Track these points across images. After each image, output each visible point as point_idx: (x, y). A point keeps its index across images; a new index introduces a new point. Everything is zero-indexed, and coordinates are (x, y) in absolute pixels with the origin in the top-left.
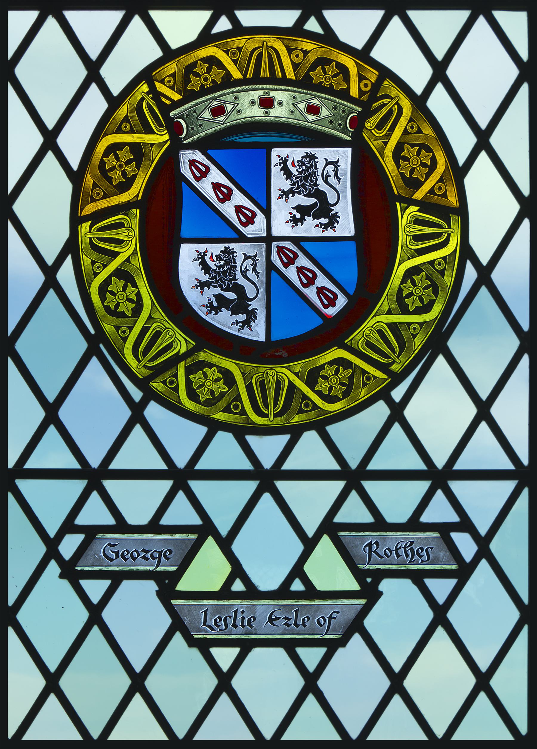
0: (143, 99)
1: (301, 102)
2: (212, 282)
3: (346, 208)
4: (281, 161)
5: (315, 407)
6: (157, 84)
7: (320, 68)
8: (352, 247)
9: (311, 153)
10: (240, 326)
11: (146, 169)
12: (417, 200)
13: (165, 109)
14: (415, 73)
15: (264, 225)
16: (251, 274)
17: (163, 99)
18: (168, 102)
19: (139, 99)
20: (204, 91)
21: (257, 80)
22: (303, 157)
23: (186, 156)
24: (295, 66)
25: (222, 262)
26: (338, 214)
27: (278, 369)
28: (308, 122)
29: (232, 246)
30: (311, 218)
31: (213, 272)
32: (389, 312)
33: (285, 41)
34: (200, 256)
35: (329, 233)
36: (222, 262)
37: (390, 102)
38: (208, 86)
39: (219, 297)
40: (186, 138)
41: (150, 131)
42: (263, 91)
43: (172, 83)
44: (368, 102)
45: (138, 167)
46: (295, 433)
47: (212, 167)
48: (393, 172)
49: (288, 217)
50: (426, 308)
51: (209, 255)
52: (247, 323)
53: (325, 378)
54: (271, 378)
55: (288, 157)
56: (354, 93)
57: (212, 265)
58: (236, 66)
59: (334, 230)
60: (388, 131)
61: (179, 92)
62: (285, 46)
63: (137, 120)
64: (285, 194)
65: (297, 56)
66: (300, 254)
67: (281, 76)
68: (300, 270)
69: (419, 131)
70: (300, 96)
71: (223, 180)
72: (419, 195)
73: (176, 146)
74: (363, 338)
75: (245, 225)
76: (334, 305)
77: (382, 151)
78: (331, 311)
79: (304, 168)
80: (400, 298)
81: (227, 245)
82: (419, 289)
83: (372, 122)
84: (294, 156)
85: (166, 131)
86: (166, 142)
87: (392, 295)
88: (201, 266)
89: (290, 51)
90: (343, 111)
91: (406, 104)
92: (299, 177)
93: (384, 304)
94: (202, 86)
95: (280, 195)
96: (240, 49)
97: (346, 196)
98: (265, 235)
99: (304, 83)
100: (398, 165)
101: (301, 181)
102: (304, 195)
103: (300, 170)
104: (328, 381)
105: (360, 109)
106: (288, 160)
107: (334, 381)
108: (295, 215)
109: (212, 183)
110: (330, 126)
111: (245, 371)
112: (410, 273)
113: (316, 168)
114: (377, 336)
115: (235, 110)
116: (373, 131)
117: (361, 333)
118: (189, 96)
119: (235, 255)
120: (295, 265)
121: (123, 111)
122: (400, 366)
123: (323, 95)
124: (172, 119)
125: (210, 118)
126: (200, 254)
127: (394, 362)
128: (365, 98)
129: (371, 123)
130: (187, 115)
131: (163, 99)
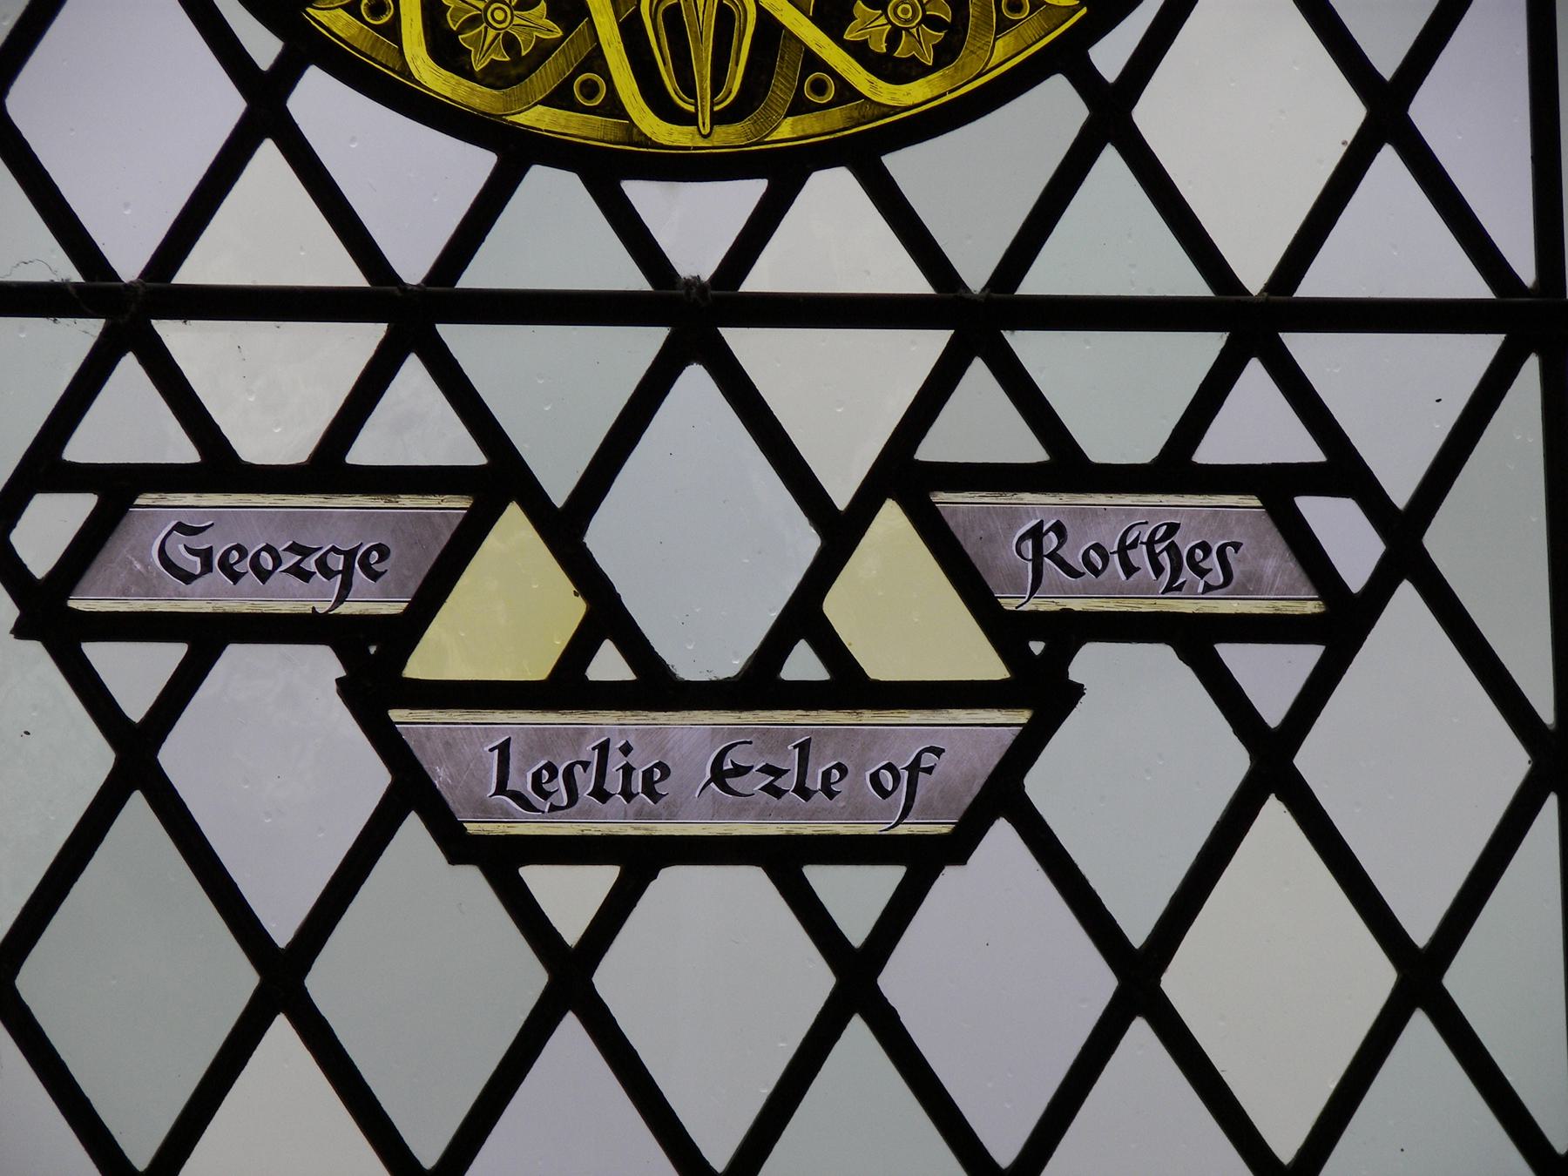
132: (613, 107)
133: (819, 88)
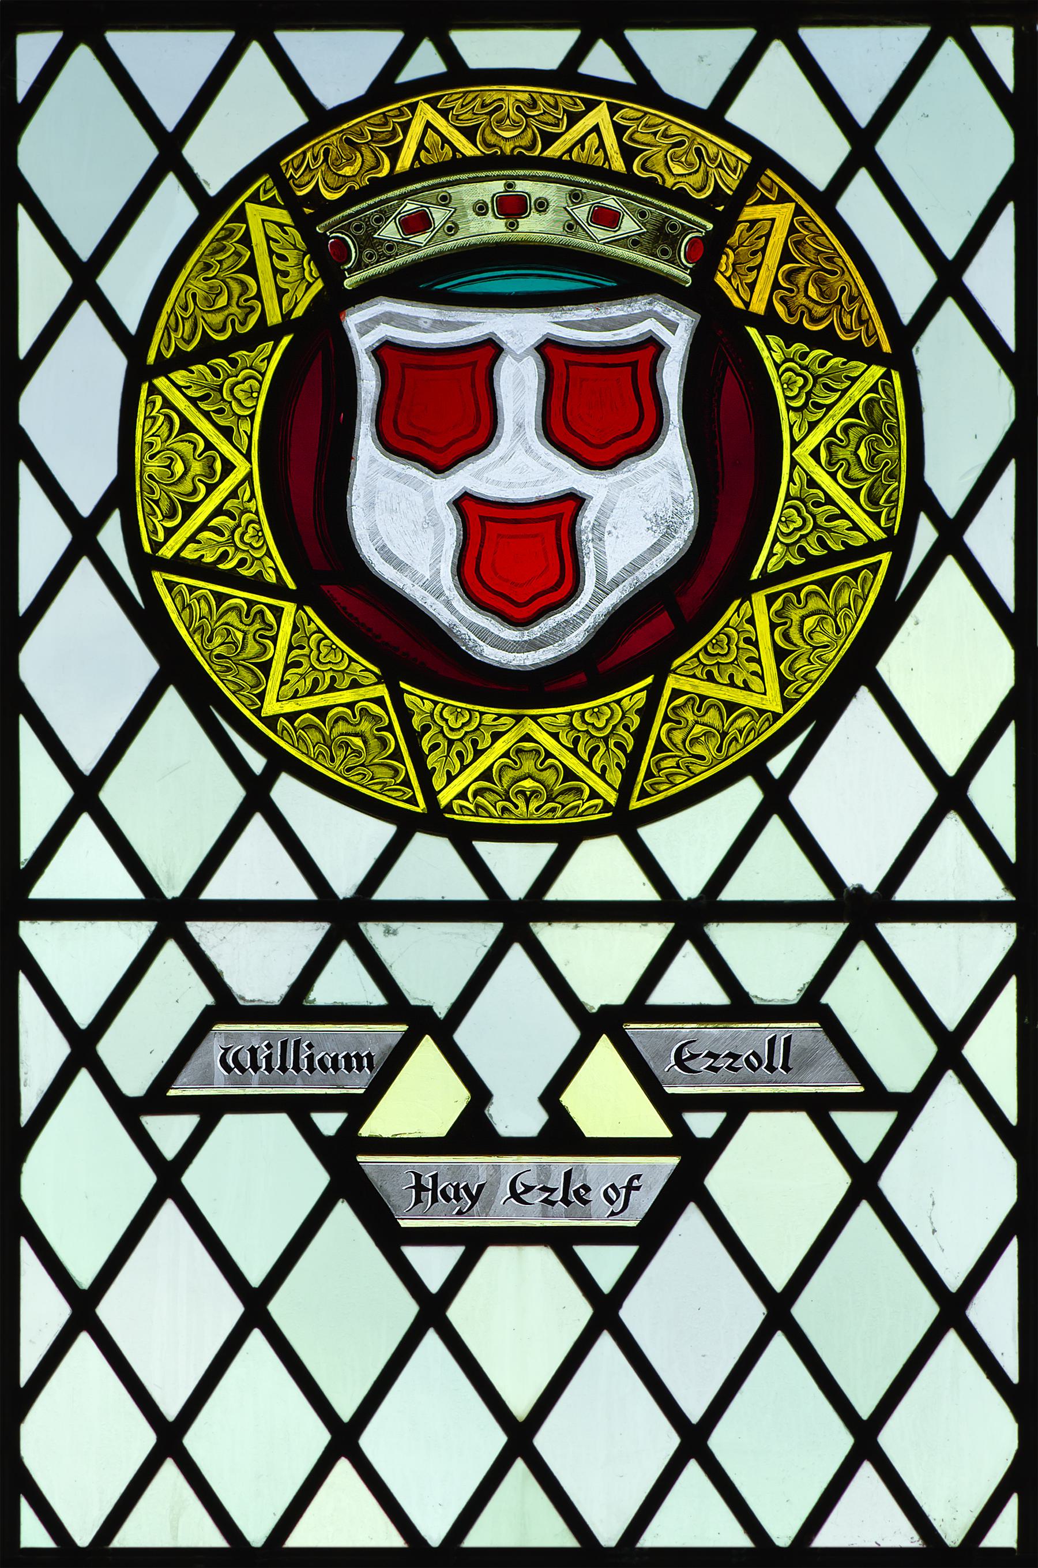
14: (815, 150)
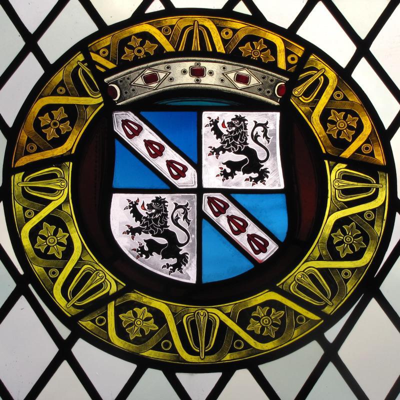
0: (78, 67)
1: (231, 72)
2: (144, 229)
3: (274, 165)
4: (212, 123)
5: (247, 346)
6: (92, 54)
7: (249, 44)
8: (281, 199)
9: (240, 116)
10: (171, 269)
11: (80, 126)
12: (345, 158)
13: (100, 76)
15: (195, 178)
16: (181, 222)
17: (98, 67)
18: (103, 70)
19: (74, 67)
20: (137, 62)
21: (188, 53)
22: (233, 119)
23: (119, 117)
24: (225, 42)
25: (154, 211)
26: (267, 170)
27: (209, 310)
28: (237, 89)
29: (163, 196)
30: (241, 173)
31: (144, 220)
32: (320, 258)
33: (215, 21)
34: (131, 205)
35: (259, 186)
36: (154, 211)
37: (316, 74)
38: (142, 57)
39: (150, 243)
40: (119, 101)
41: (84, 94)
42: (194, 62)
43: (107, 54)
44: (295, 74)
45: (72, 125)
46: (227, 371)
47: (145, 126)
48: (321, 133)
49: (219, 172)
50: (358, 255)
51: (140, 204)
52: (178, 266)
53: (257, 319)
54: (202, 318)
55: (218, 118)
56: (282, 65)
57: (144, 213)
58: (169, 41)
59: (264, 184)
60: (315, 98)
61: (114, 62)
62: (216, 25)
63: (72, 85)
64: (216, 151)
65: (227, 33)
66: (230, 204)
67: (211, 50)
68: (231, 219)
69: (345, 99)
70: (229, 68)
71: (156, 138)
72: (347, 153)
73: (110, 107)
74: (295, 282)
75: (176, 178)
76: (265, 251)
77: (309, 115)
78: (262, 257)
79: (234, 128)
80: (331, 245)
81: (158, 195)
82: (349, 237)
83: (299, 90)
84: (224, 118)
85: (100, 95)
86: (100, 104)
87: (323, 243)
88: (132, 214)
89: (220, 29)
90: (272, 81)
91: (331, 75)
92: (229, 137)
93: (315, 250)
94: (136, 57)
95: (211, 152)
96: (172, 27)
97: (275, 154)
98: (196, 186)
99: (233, 56)
100: (326, 128)
101: (231, 140)
102: (234, 153)
103: (230, 131)
104: (260, 322)
105: (287, 79)
106: (218, 122)
107: (266, 321)
108: (225, 170)
109: (145, 141)
110: (259, 93)
111: (176, 311)
112: (339, 224)
113: (246, 129)
114: (309, 280)
115: (167, 78)
116: (300, 98)
117: (293, 277)
118: (123, 65)
119: (166, 204)
120: (226, 214)
121: (58, 77)
122: (332, 309)
123: (252, 67)
124: (107, 84)
125: (143, 84)
126: (132, 203)
127: (326, 305)
128: (292, 70)
129: (298, 91)
130: (121, 81)
131: (98, 67)
132: (174, 350)
133: (239, 344)
